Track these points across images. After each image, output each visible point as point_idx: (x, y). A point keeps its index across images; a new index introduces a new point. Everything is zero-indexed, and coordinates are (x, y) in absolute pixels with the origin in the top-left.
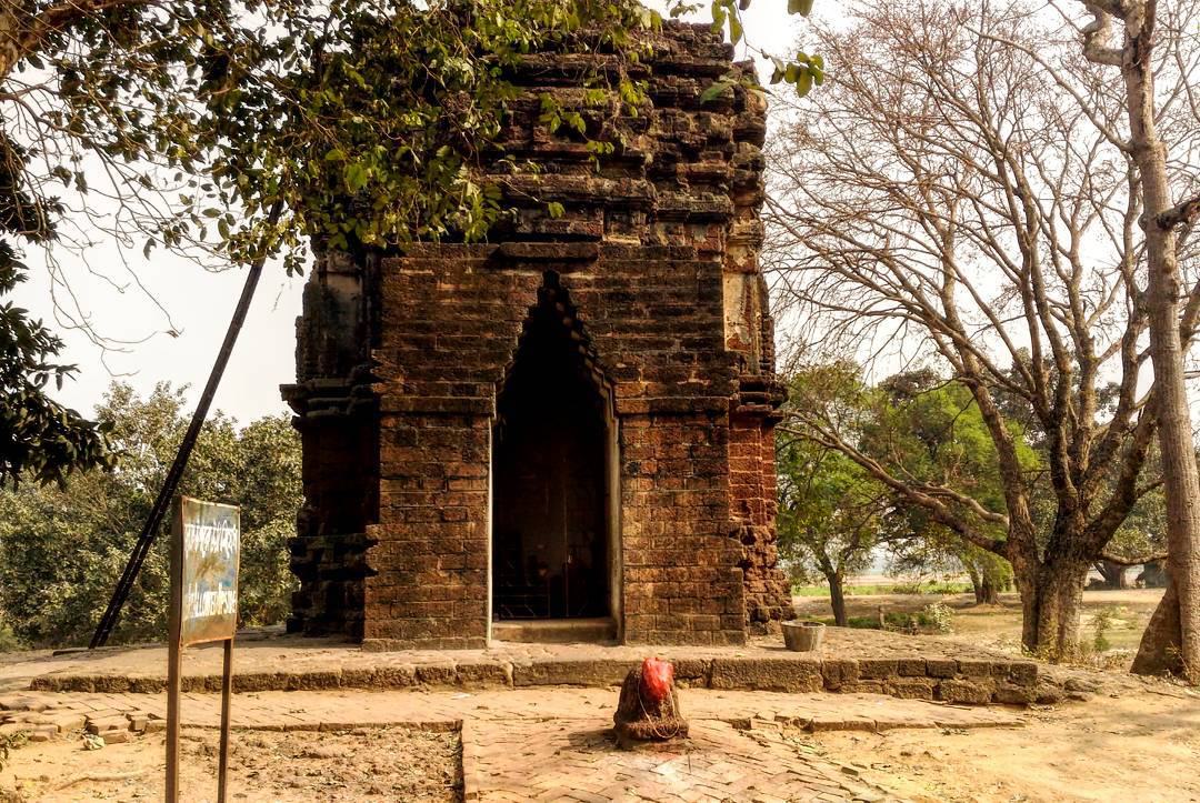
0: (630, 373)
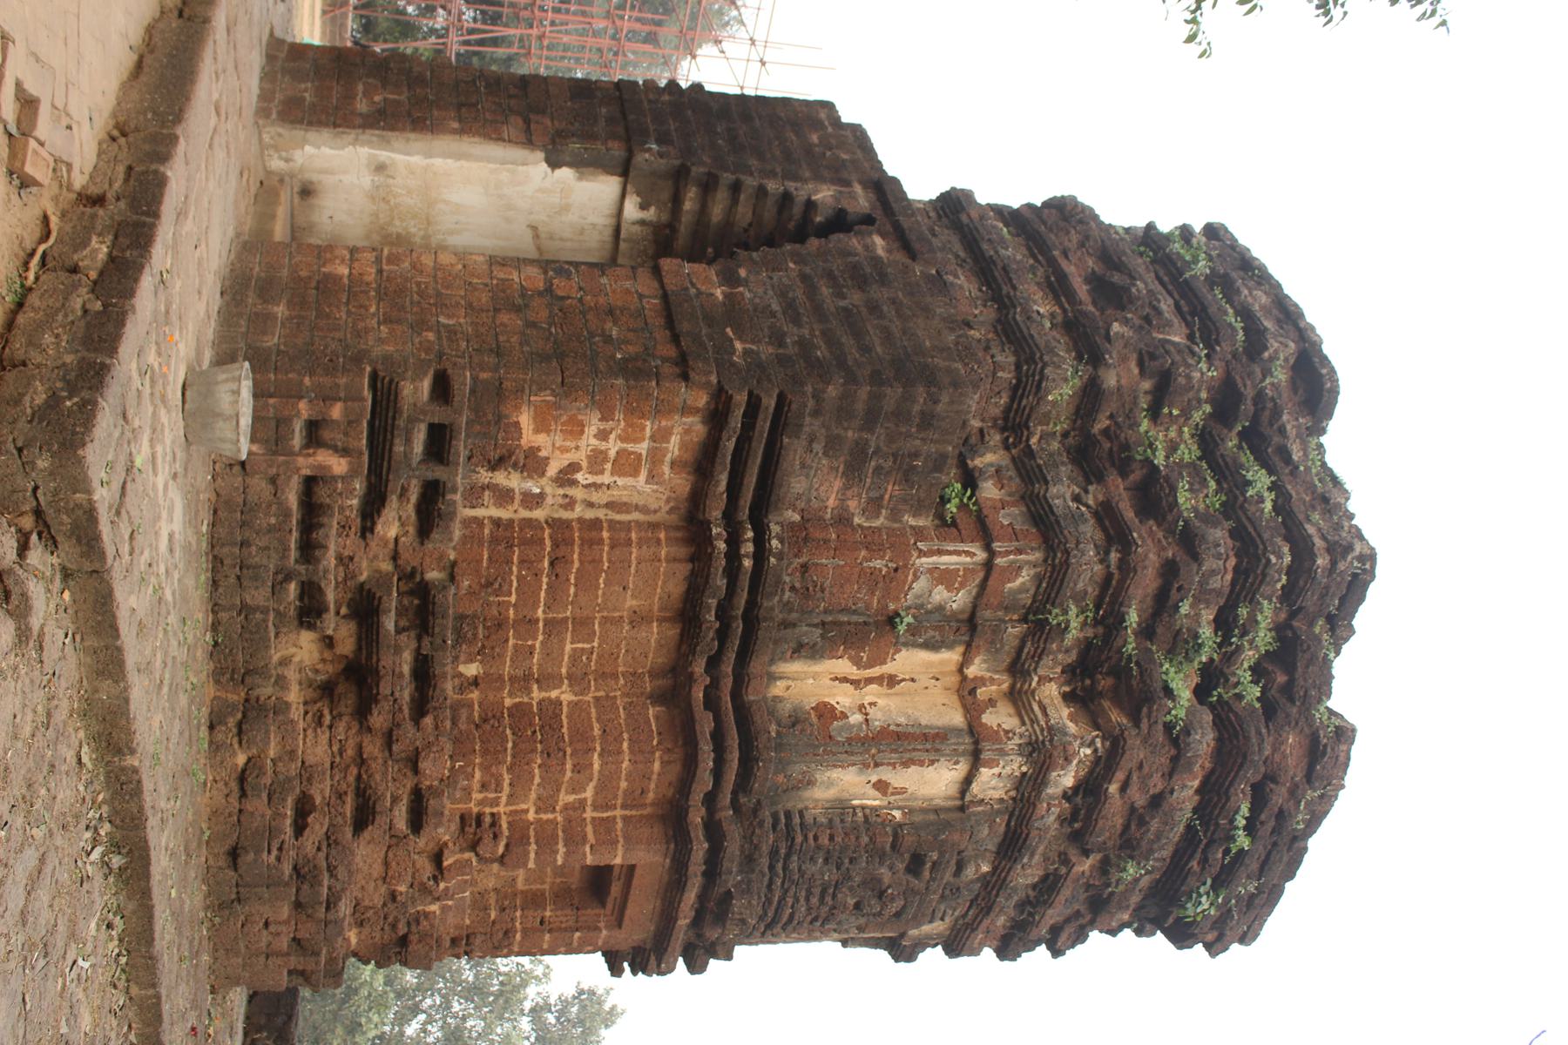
0: (730, 279)
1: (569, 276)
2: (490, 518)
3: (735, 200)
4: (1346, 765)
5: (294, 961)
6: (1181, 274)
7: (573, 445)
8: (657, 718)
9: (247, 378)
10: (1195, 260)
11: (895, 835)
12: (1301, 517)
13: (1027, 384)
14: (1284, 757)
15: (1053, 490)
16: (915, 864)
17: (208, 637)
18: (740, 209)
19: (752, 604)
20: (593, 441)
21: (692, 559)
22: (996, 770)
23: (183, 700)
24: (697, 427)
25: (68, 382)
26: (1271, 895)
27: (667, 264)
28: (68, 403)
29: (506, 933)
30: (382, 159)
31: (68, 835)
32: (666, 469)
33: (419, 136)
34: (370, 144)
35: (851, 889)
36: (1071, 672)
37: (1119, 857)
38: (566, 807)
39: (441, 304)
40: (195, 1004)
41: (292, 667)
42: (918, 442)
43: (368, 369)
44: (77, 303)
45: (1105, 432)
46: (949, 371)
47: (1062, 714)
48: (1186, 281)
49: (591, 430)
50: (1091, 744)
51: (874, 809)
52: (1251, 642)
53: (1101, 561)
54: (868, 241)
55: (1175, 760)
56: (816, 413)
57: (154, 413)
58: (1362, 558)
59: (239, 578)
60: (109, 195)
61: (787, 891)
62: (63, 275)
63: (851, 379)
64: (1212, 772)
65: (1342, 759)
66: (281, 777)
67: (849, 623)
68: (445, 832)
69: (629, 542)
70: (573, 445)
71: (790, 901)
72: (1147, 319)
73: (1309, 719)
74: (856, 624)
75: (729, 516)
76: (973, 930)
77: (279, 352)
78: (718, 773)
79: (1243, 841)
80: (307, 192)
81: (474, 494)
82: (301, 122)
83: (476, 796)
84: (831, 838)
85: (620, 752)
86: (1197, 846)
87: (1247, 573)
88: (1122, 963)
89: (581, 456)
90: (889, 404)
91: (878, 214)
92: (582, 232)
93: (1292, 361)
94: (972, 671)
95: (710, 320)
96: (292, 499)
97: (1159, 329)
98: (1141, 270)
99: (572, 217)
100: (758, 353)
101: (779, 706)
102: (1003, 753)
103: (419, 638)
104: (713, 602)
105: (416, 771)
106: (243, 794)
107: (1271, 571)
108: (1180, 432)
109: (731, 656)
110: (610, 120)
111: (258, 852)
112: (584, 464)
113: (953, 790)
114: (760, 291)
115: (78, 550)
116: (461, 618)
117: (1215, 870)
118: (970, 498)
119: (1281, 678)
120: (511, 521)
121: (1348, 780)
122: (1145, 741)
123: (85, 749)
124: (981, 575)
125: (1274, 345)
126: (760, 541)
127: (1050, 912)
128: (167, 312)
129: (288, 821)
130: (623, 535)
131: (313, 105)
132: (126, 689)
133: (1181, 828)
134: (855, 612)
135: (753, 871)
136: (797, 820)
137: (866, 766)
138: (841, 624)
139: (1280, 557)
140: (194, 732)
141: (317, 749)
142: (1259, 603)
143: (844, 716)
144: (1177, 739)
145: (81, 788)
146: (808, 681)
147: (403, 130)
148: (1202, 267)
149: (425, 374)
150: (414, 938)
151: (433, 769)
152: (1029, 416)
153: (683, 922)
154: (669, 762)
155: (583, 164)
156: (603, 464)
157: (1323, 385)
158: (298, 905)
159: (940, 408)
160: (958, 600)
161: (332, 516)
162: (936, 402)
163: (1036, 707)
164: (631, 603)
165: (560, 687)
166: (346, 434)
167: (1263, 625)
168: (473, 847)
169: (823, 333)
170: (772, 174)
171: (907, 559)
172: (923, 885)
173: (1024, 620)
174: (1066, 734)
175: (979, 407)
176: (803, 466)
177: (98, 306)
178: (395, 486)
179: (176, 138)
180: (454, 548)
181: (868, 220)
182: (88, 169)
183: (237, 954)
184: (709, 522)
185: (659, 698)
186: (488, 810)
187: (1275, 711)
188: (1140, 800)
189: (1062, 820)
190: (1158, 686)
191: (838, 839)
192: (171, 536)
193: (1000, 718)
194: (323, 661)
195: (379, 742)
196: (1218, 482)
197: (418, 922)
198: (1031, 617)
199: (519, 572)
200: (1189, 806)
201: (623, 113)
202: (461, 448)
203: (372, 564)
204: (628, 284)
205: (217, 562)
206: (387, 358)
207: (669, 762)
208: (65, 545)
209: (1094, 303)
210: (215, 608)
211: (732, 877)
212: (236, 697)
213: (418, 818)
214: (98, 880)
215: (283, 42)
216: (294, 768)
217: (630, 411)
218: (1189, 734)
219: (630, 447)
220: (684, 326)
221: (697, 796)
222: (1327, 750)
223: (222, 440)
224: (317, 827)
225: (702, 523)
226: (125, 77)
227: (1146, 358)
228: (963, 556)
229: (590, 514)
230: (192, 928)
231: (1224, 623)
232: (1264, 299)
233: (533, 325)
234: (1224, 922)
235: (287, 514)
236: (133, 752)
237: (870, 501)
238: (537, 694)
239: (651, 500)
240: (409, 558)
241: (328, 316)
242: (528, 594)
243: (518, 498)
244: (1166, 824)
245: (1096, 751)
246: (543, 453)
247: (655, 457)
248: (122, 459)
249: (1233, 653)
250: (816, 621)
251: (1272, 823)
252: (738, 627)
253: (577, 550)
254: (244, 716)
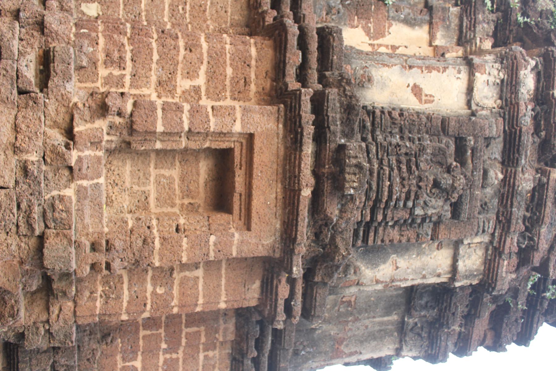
29: (145, 241)
83: (103, 72)
150: (50, 232)
197: (53, 206)
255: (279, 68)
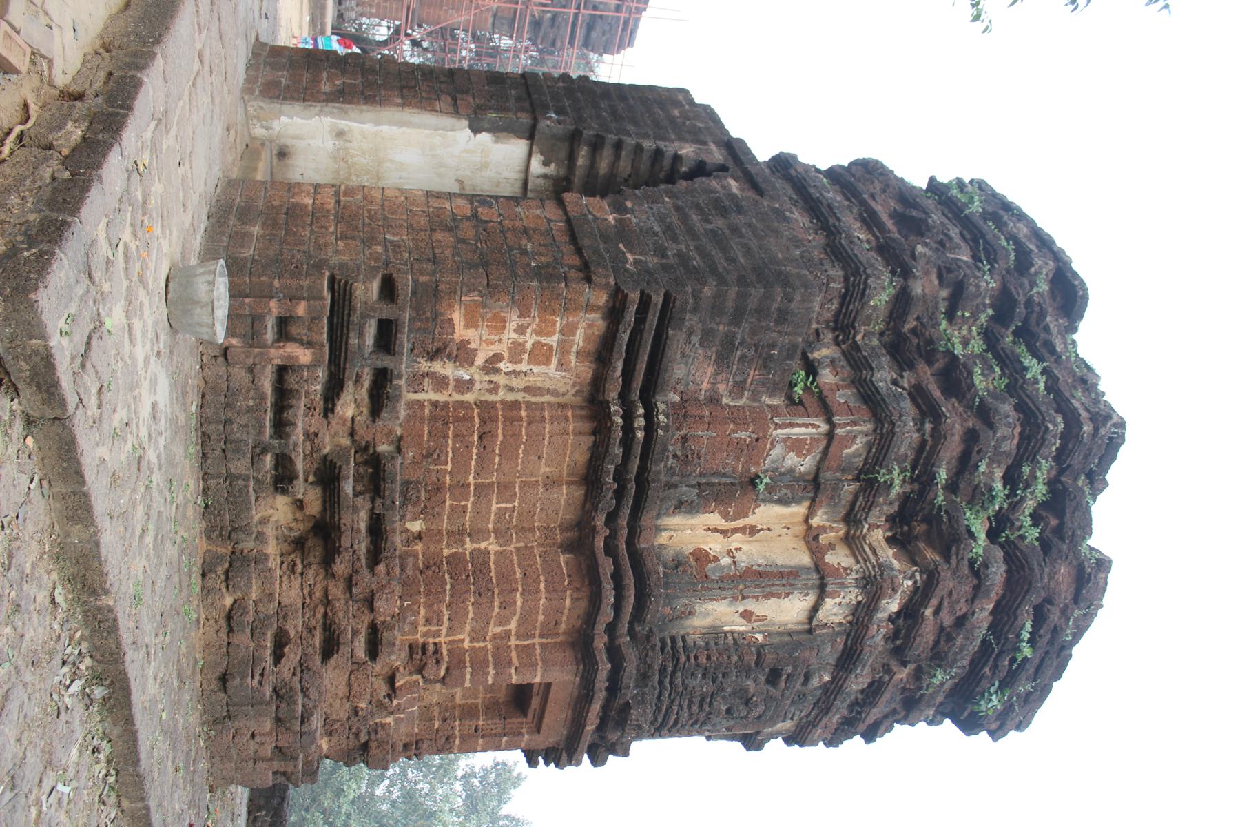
0: (619, 208)
1: (491, 206)
2: (429, 401)
3: (617, 156)
4: (1105, 589)
5: (276, 765)
6: (962, 212)
7: (497, 338)
8: (567, 563)
9: (222, 275)
10: (971, 200)
11: (759, 654)
12: (1067, 394)
13: (854, 290)
14: (1058, 584)
15: (878, 375)
16: (774, 676)
17: (200, 500)
18: (622, 163)
19: (643, 469)
20: (514, 335)
21: (594, 433)
22: (837, 600)
23: (171, 551)
24: (597, 321)
25: (29, 237)
26: (1043, 692)
27: (567, 197)
28: (26, 254)
29: (447, 739)
30: (342, 126)
31: (38, 671)
32: (573, 358)
33: (371, 108)
34: (331, 114)
35: (724, 698)
36: (893, 520)
37: (930, 666)
38: (494, 637)
39: (387, 225)
40: (192, 804)
41: (270, 525)
42: (775, 335)
43: (327, 274)
44: (47, 173)
45: (913, 331)
46: (799, 276)
47: (888, 554)
48: (966, 216)
49: (511, 326)
50: (912, 577)
51: (741, 633)
52: (1032, 493)
53: (918, 431)
54: (725, 182)
55: (976, 588)
56: (695, 310)
57: (129, 287)
58: (1115, 425)
59: (224, 450)
60: (88, 92)
61: (673, 701)
62: (36, 151)
63: (722, 281)
64: (1003, 596)
65: (1101, 584)
66: (261, 616)
67: (720, 484)
68: (396, 659)
69: (543, 419)
70: (497, 338)
71: (675, 708)
72: (942, 243)
73: (1077, 553)
74: (725, 484)
75: (624, 396)
76: (814, 727)
77: (254, 261)
78: (617, 607)
79: (1027, 651)
80: (283, 154)
81: (416, 381)
82: (278, 97)
83: (422, 629)
84: (709, 658)
85: (538, 591)
86: (990, 656)
87: (1029, 438)
88: (923, 750)
89: (503, 348)
90: (752, 303)
91: (730, 164)
92: (498, 184)
93: (1051, 276)
94: (816, 521)
95: (605, 238)
96: (267, 385)
97: (952, 250)
98: (932, 207)
99: (489, 173)
100: (646, 262)
101: (664, 552)
102: (843, 586)
103: (373, 500)
104: (612, 468)
105: (372, 609)
106: (231, 630)
107: (1049, 437)
108: (970, 330)
109: (626, 512)
110: (518, 99)
111: (243, 677)
112: (506, 355)
113: (803, 616)
114: (644, 217)
115: (40, 397)
116: (407, 483)
117: (1003, 674)
118: (812, 383)
119: (1054, 522)
120: (447, 403)
121: (1105, 601)
122: (954, 573)
123: (59, 589)
124: (824, 443)
125: (1038, 262)
126: (650, 416)
127: (874, 710)
128: (145, 202)
129: (269, 652)
130: (538, 413)
131: (288, 87)
132: (95, 533)
133: (977, 643)
134: (724, 475)
135: (646, 685)
136: (680, 644)
137: (735, 599)
138: (714, 484)
139: (1055, 425)
140: (184, 578)
141: (291, 593)
142: (1038, 462)
143: (716, 559)
144: (978, 572)
145: (56, 626)
146: (685, 532)
147: (358, 103)
148: (976, 207)
149: (374, 277)
150: (373, 744)
151: (386, 607)
152: (855, 318)
153: (590, 728)
154: (578, 599)
155: (497, 130)
156: (520, 357)
157: (1076, 293)
158: (278, 720)
159: (793, 305)
160: (805, 464)
161: (300, 398)
162: (790, 301)
163: (867, 549)
164: (544, 469)
165: (488, 539)
166: (310, 330)
167: (1040, 480)
168: (420, 670)
169: (697, 248)
170: (646, 136)
171: (766, 431)
172: (779, 693)
173: (857, 479)
174: (893, 569)
175: (821, 307)
176: (683, 355)
177: (67, 175)
178: (351, 373)
179: (155, 54)
180: (400, 425)
181: (723, 168)
182: (72, 71)
183: (230, 760)
184: (608, 402)
185: (568, 547)
186: (431, 640)
187: (1050, 548)
188: (947, 619)
189: (887, 639)
190: (963, 529)
191: (714, 658)
192: (154, 406)
193: (839, 558)
194: (296, 520)
195: (341, 586)
196: (1001, 369)
198: (862, 476)
199: (454, 444)
200: (985, 625)
201: (529, 95)
202: (405, 340)
203: (333, 439)
204: (538, 212)
205: (206, 437)
206: (342, 265)
207: (578, 599)
208: (26, 392)
209: (900, 233)
210: (205, 477)
211: (630, 691)
212: (224, 550)
213: (373, 650)
214: (79, 711)
215: (266, 44)
216: (272, 608)
217: (543, 309)
218: (987, 568)
219: (543, 339)
220: (585, 242)
221: (600, 627)
222: (1089, 578)
223: (200, 325)
224: (293, 655)
225: (601, 403)
226: (114, 11)
227: (944, 271)
228: (810, 428)
229: (510, 397)
230: (189, 742)
231: (1011, 479)
232: (1025, 230)
233: (463, 241)
234: (1007, 714)
235: (263, 398)
236: (107, 592)
237: (736, 384)
238: (469, 545)
239: (560, 385)
240: (363, 434)
241: (295, 234)
242: (461, 465)
243: (452, 384)
244: (968, 639)
245: (915, 582)
246: (472, 346)
247: (564, 347)
248: (87, 316)
249: (1017, 503)
250: (693, 483)
251: (1048, 637)
252: (632, 487)
253: (501, 426)
254: (231, 565)
255: (590, 617)
